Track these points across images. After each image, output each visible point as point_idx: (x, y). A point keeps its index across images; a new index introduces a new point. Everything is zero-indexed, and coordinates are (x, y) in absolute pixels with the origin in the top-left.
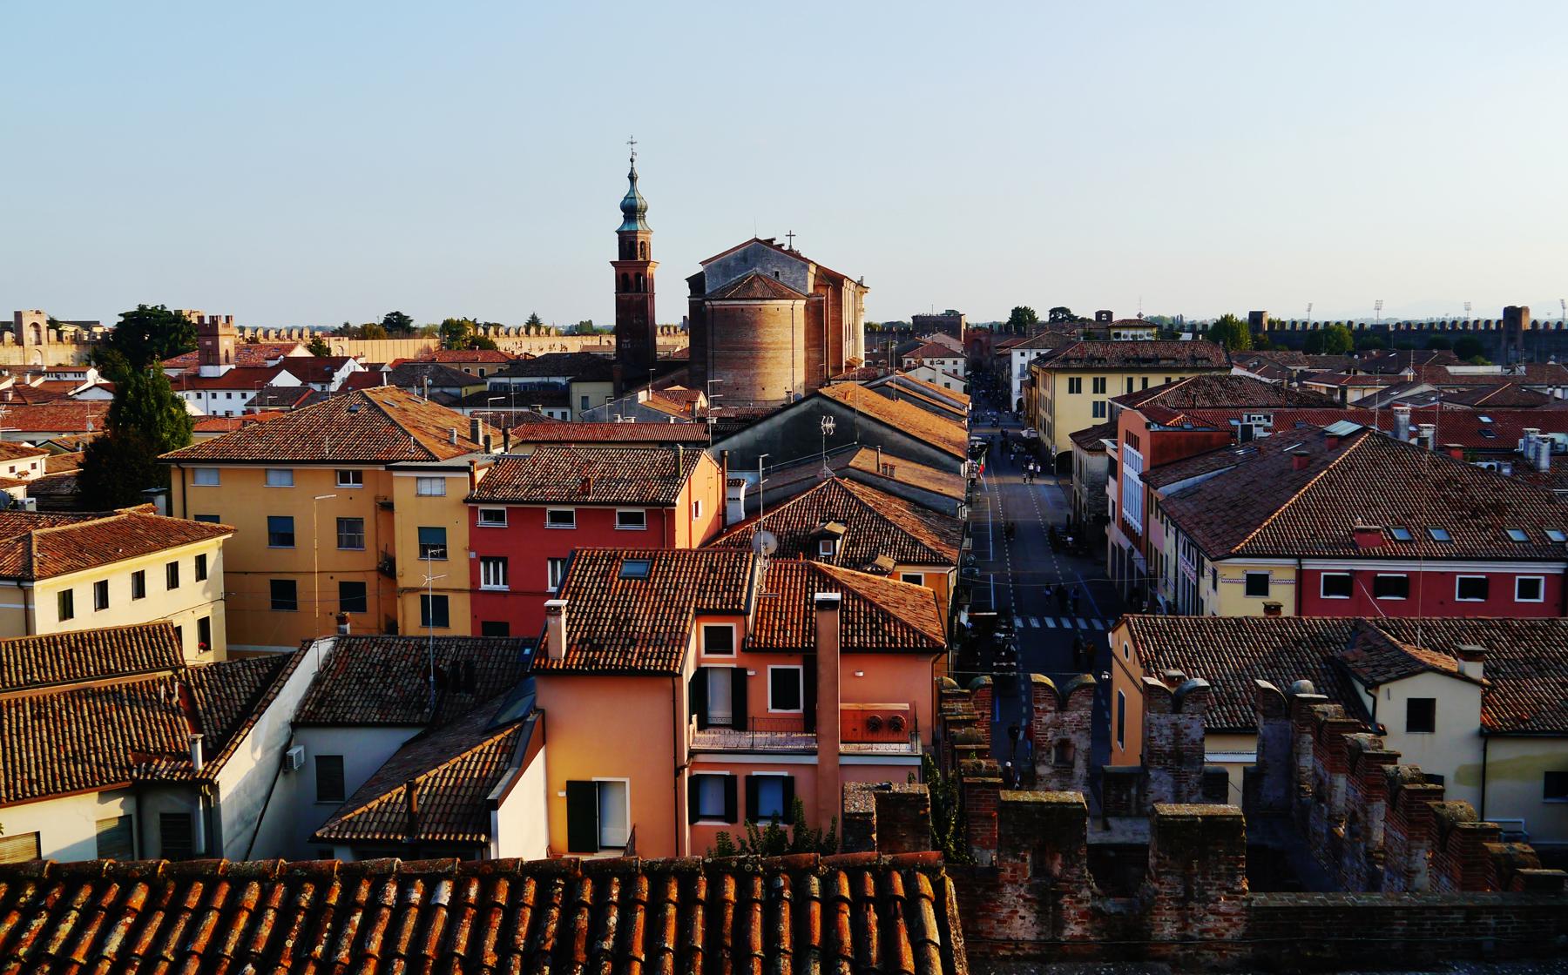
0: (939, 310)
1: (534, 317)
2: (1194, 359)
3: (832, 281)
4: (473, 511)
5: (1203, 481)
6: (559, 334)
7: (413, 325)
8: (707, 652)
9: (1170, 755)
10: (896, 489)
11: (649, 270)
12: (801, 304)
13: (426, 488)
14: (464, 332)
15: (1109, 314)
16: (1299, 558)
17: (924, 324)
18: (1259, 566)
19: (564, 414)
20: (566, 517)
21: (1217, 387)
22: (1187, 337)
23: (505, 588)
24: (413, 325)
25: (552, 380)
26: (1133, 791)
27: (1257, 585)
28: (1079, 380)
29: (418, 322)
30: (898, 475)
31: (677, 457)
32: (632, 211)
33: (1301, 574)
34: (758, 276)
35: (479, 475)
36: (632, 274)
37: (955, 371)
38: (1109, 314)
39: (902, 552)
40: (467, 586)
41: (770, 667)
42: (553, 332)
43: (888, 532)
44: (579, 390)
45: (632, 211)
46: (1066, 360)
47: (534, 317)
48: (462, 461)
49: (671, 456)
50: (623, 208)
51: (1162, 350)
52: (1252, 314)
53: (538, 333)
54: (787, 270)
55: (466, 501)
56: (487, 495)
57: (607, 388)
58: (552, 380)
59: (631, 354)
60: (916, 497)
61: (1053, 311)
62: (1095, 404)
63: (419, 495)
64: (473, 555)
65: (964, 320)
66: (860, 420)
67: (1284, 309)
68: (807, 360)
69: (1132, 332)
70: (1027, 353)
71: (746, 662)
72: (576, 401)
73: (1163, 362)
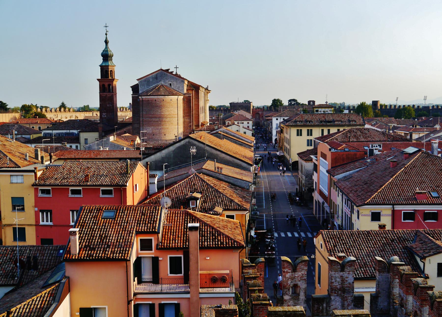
0: (241, 100)
1: (63, 104)
2: (349, 121)
3: (195, 88)
4: (36, 190)
5: (353, 173)
6: (74, 111)
7: (8, 107)
8: (141, 250)
9: (340, 290)
10: (223, 178)
11: (114, 83)
12: (181, 97)
13: (14, 180)
14: (31, 110)
15: (314, 102)
16: (393, 205)
17: (234, 106)
18: (376, 209)
19: (77, 147)
20: (78, 192)
21: (359, 133)
22: (346, 112)
23: (51, 224)
24: (8, 107)
25: (71, 131)
26: (325, 305)
27: (376, 217)
28: (301, 130)
29: (10, 105)
30: (224, 172)
31: (127, 165)
32: (106, 56)
33: (394, 211)
34: (162, 85)
35: (39, 174)
36: (106, 84)
37: (248, 127)
38: (314, 102)
39: (226, 205)
40: (34, 223)
41: (169, 256)
42: (71, 110)
43: (220, 197)
44: (83, 136)
45: (106, 56)
46: (296, 122)
47: (63, 104)
48: (31, 168)
49: (124, 165)
50: (103, 55)
51: (336, 117)
52: (373, 102)
53: (65, 111)
54: (175, 83)
55: (33, 185)
56: (42, 182)
57: (96, 135)
58: (71, 131)
59: (107, 121)
60: (232, 181)
61: (290, 101)
62: (308, 140)
63: (12, 183)
64: (36, 209)
65: (252, 104)
66: (207, 148)
67: (386, 100)
68: (184, 122)
69: (323, 110)
70: (279, 118)
71: (158, 254)
72: (82, 140)
73: (336, 123)
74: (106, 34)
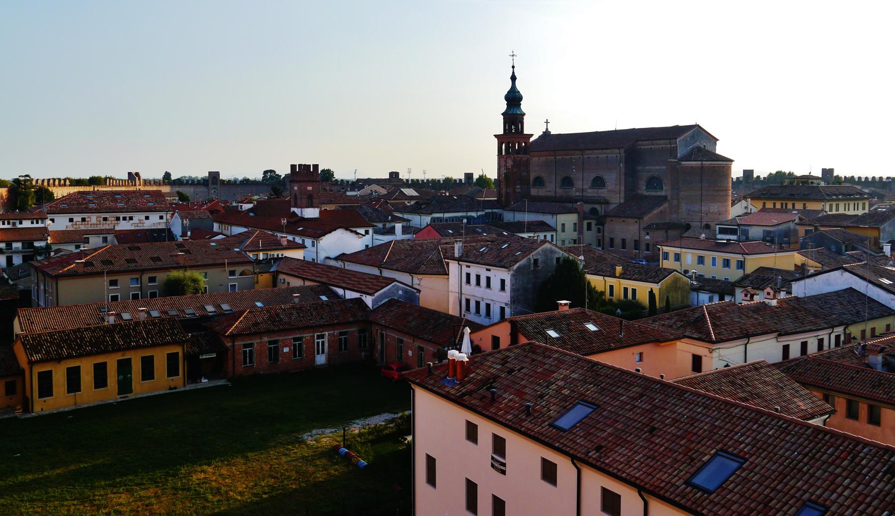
32: (514, 98)
38: (397, 174)
42: (68, 183)
45: (514, 98)
52: (745, 171)
72: (559, 228)
74: (513, 67)
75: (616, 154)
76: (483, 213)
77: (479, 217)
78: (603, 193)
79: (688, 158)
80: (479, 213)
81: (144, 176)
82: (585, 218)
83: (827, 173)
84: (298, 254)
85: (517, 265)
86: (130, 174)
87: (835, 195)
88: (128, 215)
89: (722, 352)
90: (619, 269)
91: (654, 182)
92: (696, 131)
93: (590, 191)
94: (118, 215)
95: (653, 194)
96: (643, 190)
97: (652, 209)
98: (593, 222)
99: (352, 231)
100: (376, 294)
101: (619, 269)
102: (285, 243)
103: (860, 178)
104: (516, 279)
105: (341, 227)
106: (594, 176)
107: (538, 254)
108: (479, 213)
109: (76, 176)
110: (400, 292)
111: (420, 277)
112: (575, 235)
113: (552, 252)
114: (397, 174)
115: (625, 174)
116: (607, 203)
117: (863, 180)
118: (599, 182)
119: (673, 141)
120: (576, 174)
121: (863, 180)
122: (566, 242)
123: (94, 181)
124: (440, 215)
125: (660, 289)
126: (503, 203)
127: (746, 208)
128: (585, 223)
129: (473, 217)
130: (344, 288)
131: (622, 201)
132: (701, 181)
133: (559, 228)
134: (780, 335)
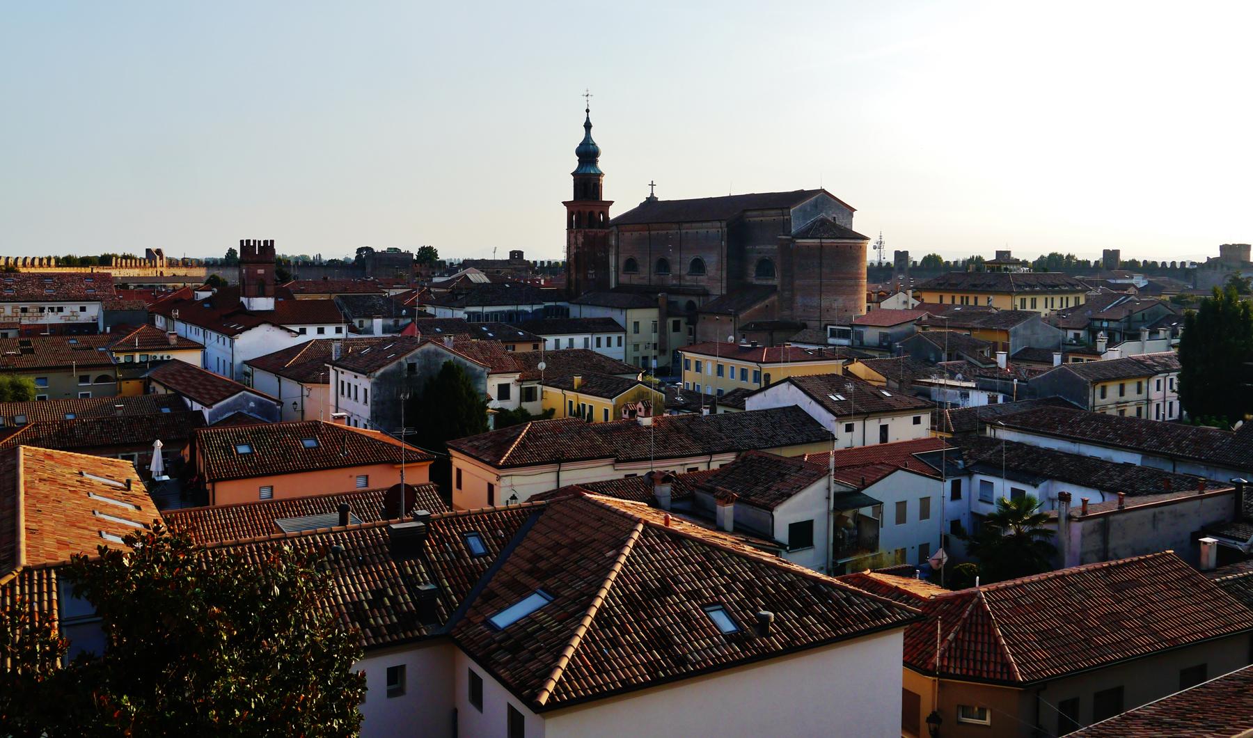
25: (521, 308)
32: (588, 153)
38: (520, 253)
45: (588, 153)
50: (578, 153)
58: (521, 308)
72: (630, 327)
74: (588, 111)
75: (715, 229)
76: (541, 307)
77: (535, 312)
78: (702, 281)
79: (804, 234)
80: (535, 307)
81: (166, 254)
82: (669, 315)
83: (1111, 256)
84: (192, 358)
85: (382, 370)
86: (148, 251)
87: (1030, 286)
88: (56, 305)
89: (516, 480)
90: (577, 380)
91: (765, 268)
92: (822, 199)
93: (688, 278)
94: (41, 304)
95: (764, 282)
96: (752, 278)
97: (754, 302)
98: (683, 321)
99: (282, 328)
100: (215, 406)
101: (577, 380)
102: (173, 341)
103: (956, 262)
104: (379, 389)
105: (265, 322)
106: (691, 257)
107: (415, 356)
108: (535, 307)
109: (79, 254)
110: (252, 404)
111: (309, 386)
112: (654, 338)
113: (437, 354)
114: (520, 253)
115: (728, 256)
116: (706, 294)
117: (1178, 266)
118: (698, 266)
119: (786, 211)
120: (673, 256)
121: (1178, 266)
122: (641, 347)
123: (106, 260)
124: (478, 309)
125: (615, 407)
126: (570, 294)
127: (905, 303)
128: (670, 321)
129: (526, 312)
130: (191, 399)
131: (724, 292)
132: (821, 265)
133: (630, 327)
134: (618, 461)
